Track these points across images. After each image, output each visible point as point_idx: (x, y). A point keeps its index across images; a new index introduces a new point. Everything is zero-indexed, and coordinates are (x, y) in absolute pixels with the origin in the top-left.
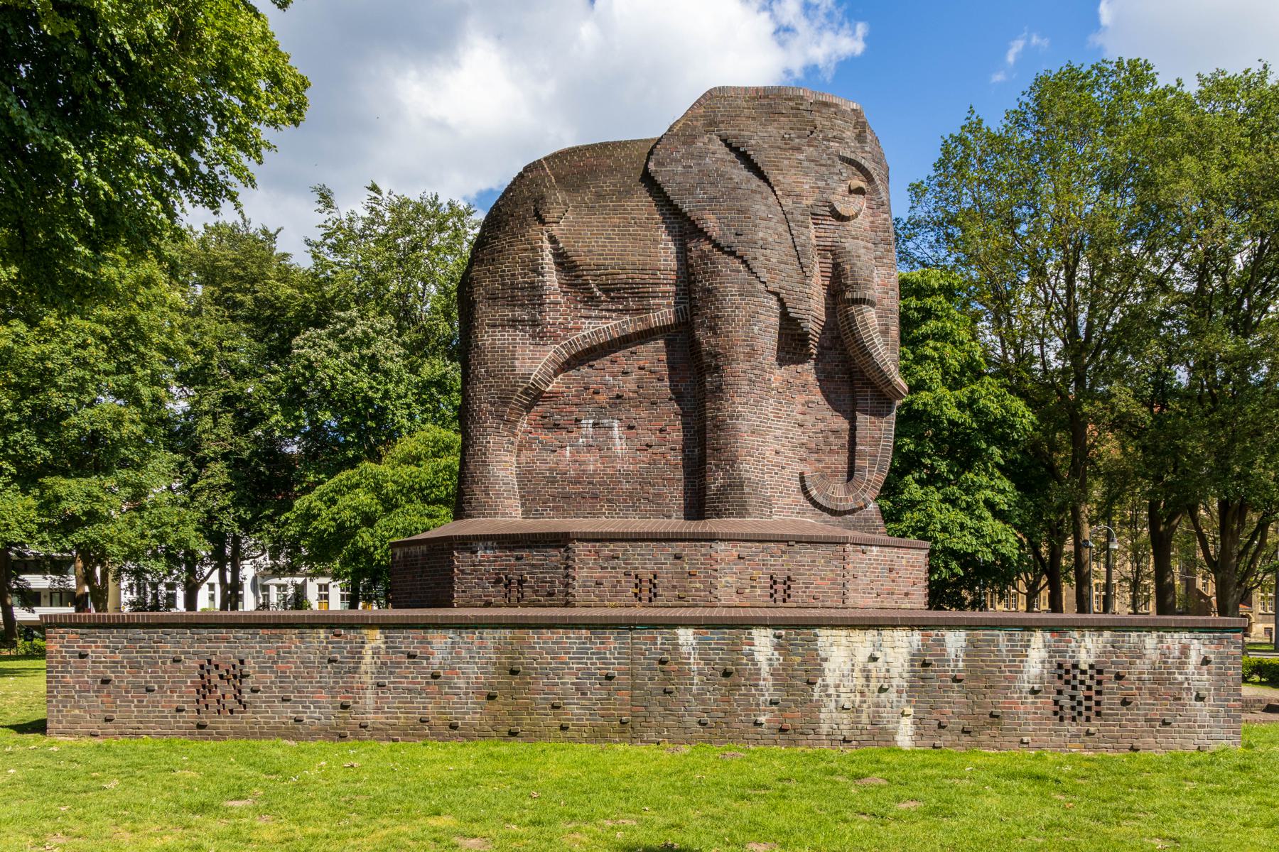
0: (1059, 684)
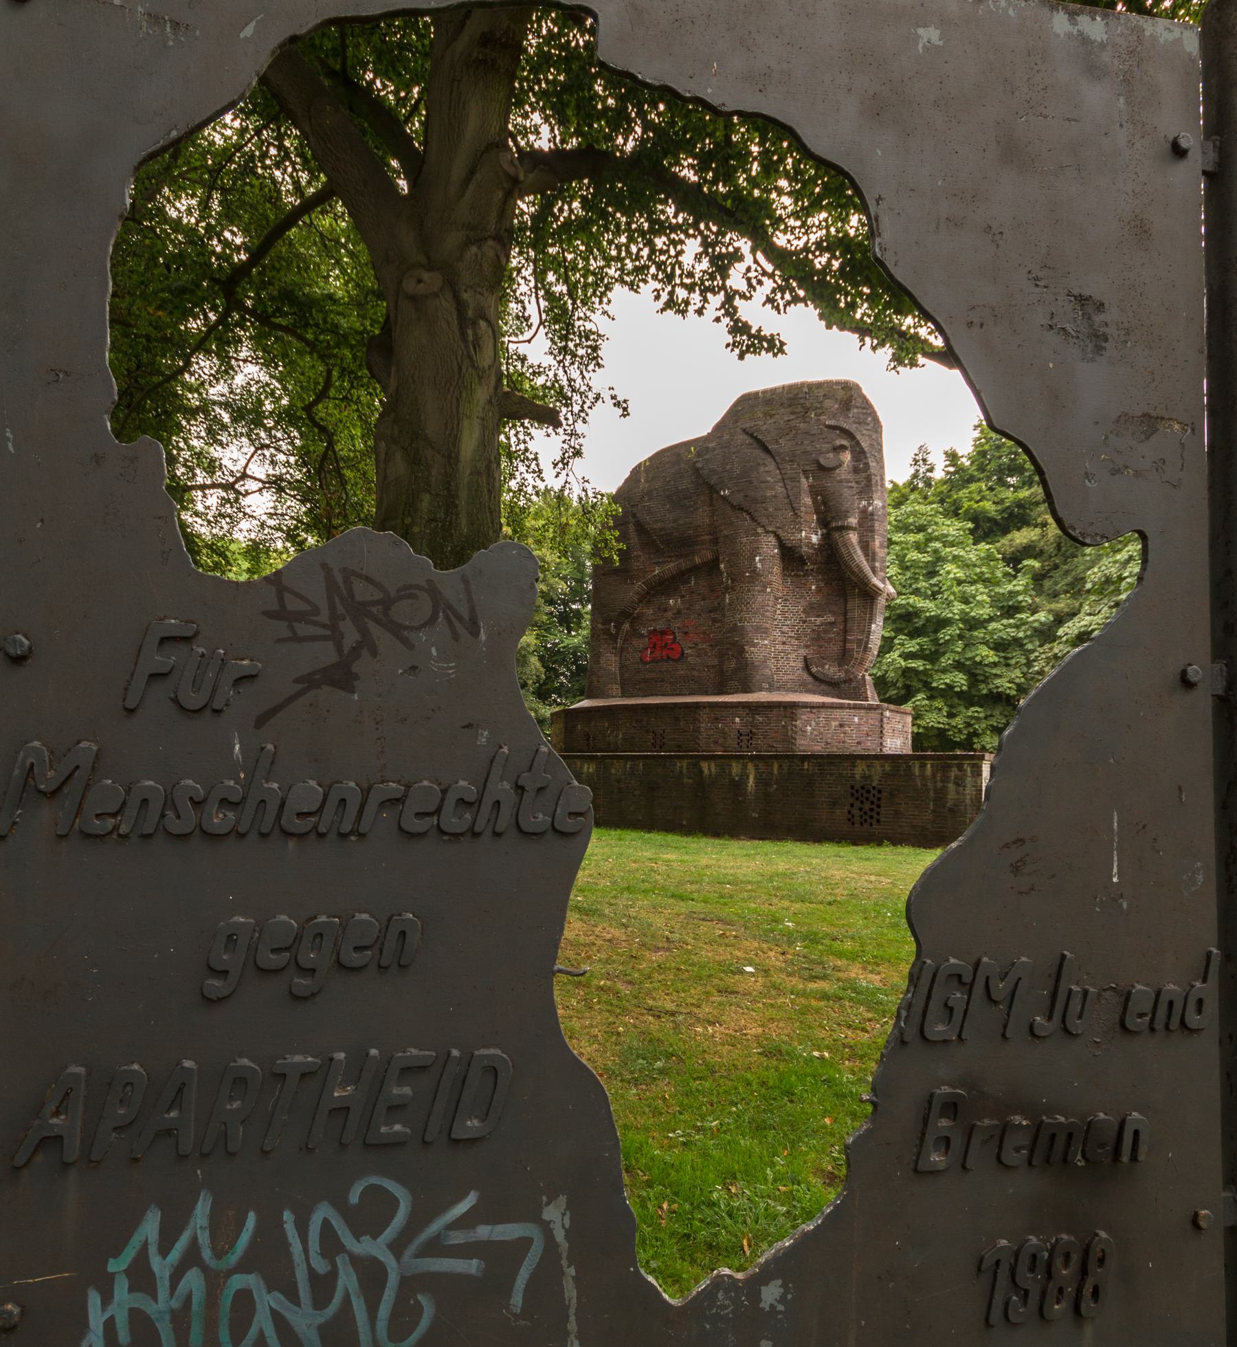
0: (851, 800)
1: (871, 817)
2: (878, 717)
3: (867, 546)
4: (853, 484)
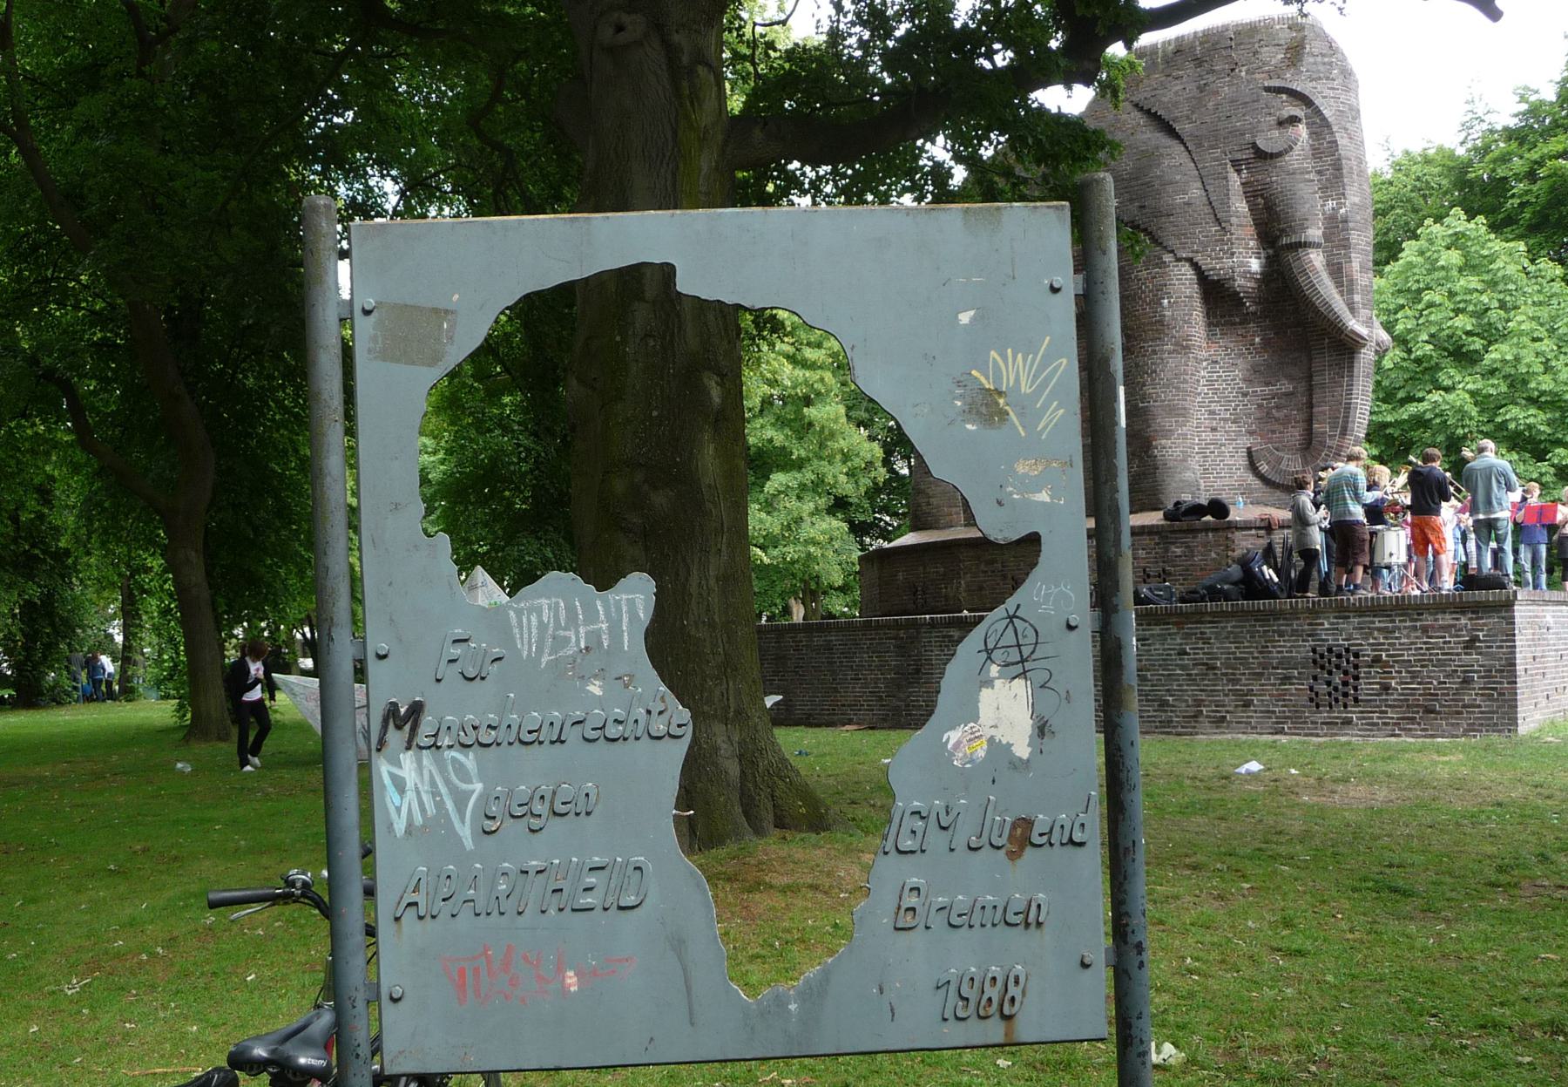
1: (1346, 695)
3: (1340, 270)
4: (1312, 176)
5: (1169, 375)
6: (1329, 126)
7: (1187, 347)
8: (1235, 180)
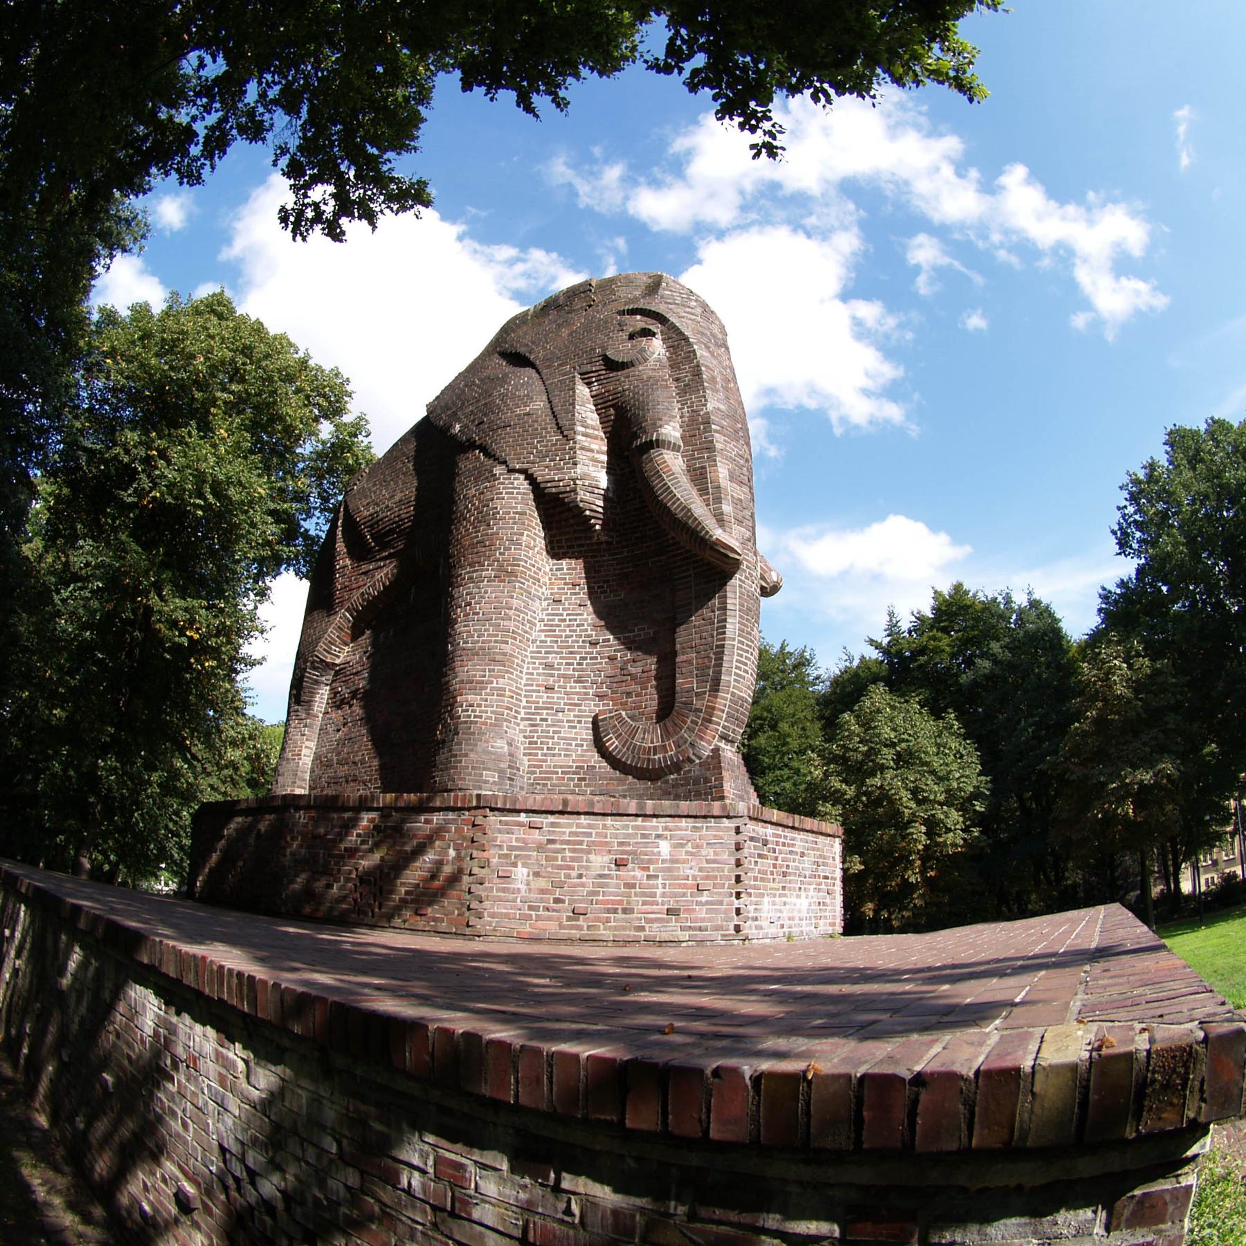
2: (731, 839)
5: (487, 608)
6: (686, 339)
7: (513, 574)
8: (582, 391)
